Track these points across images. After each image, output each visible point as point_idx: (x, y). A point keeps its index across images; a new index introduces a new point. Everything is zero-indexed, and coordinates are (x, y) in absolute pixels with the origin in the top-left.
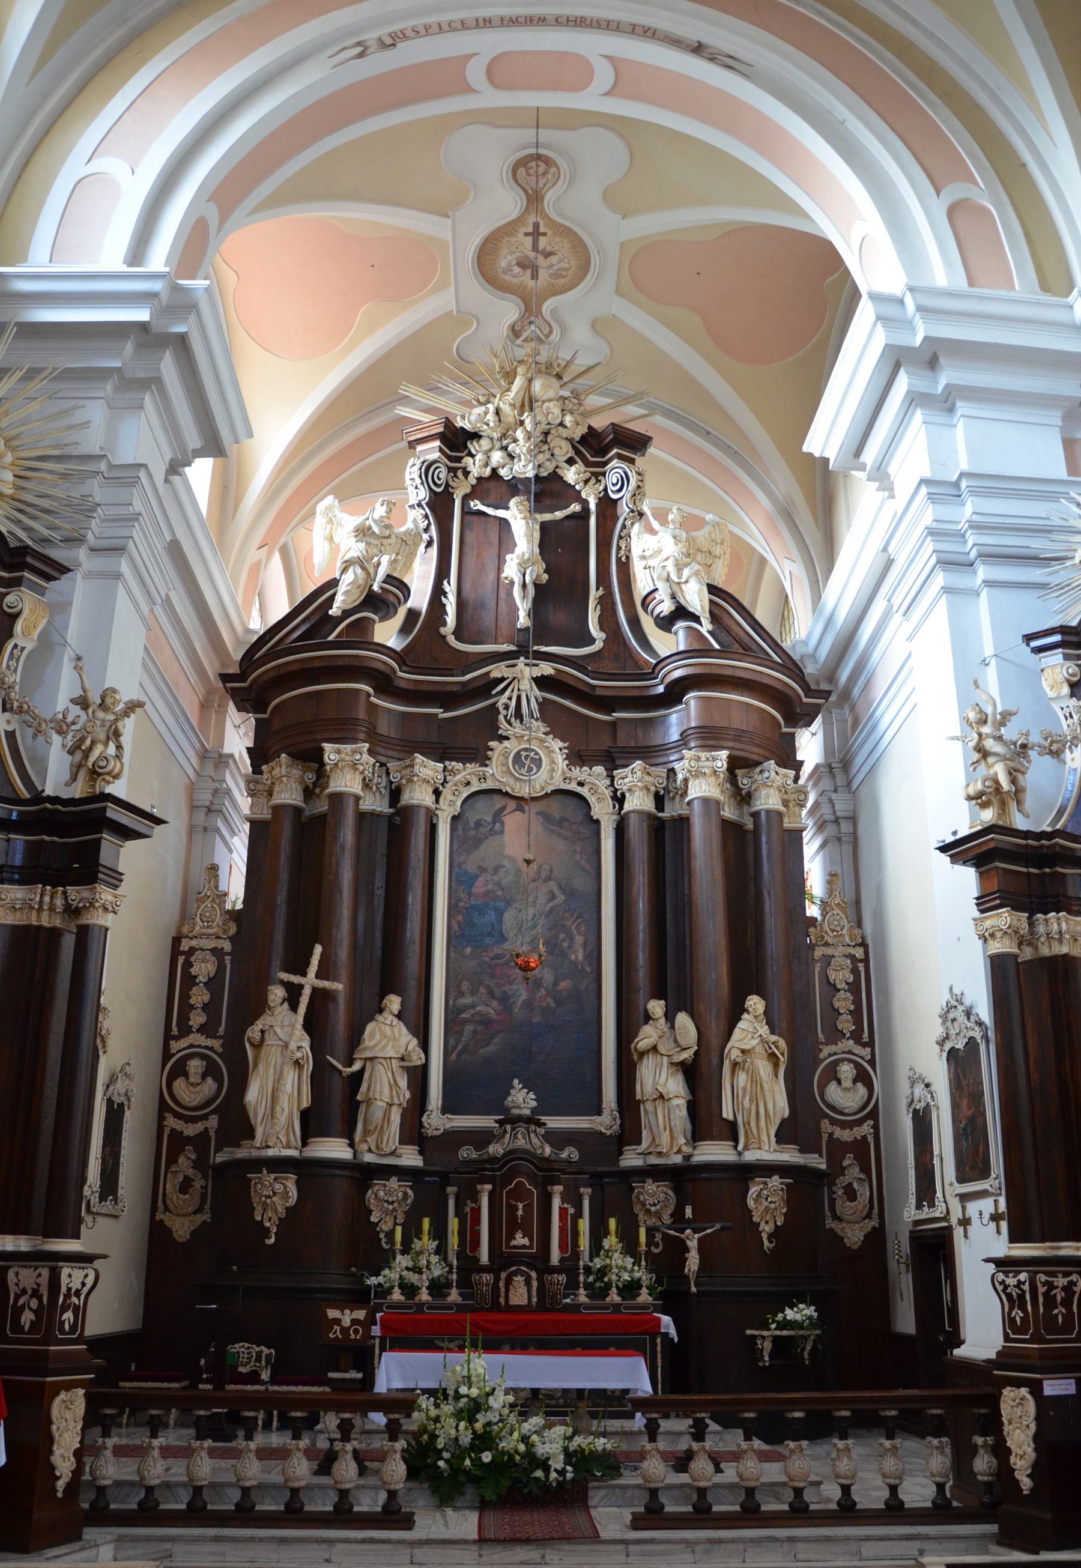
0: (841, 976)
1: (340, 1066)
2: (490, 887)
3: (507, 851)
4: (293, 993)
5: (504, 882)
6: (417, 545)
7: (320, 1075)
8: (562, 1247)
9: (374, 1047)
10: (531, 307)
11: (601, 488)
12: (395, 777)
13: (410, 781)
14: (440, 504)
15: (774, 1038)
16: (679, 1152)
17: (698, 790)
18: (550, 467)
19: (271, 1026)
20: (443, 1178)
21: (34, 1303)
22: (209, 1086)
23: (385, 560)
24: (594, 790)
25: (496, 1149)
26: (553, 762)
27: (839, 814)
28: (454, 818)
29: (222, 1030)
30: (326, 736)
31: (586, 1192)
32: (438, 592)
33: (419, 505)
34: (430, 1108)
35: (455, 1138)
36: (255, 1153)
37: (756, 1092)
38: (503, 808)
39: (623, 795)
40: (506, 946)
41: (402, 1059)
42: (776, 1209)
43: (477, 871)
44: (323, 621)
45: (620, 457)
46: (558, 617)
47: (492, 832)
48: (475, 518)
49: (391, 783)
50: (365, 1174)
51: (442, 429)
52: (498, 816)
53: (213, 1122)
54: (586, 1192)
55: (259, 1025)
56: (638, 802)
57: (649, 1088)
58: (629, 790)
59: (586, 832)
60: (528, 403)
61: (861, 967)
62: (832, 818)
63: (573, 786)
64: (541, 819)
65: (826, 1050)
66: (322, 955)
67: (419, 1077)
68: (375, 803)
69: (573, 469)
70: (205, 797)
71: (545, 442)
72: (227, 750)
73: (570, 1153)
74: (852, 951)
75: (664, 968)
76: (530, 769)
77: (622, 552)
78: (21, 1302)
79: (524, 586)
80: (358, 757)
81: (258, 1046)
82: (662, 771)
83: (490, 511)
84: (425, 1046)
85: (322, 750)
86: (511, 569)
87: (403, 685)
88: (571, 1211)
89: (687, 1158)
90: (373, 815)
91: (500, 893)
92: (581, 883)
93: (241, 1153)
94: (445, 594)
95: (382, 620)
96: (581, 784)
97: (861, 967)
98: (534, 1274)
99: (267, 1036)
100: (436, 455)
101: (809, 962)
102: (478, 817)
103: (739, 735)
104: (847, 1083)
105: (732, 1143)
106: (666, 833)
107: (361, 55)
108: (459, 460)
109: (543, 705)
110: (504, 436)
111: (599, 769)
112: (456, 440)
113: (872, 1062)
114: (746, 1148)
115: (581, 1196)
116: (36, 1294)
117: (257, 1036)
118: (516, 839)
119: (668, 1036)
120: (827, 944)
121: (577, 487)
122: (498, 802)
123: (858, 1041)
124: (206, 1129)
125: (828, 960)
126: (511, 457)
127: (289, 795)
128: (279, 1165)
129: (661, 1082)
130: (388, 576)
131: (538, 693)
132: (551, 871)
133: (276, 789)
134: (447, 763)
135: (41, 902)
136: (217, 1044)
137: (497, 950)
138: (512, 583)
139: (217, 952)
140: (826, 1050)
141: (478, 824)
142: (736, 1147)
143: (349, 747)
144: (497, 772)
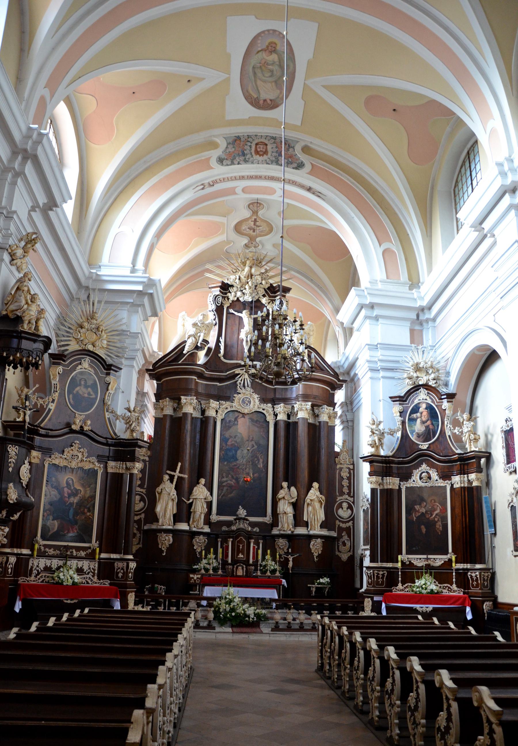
0: (345, 474)
1: (186, 501)
2: (233, 442)
3: (239, 431)
7: (180, 504)
8: (253, 558)
10: (252, 239)
12: (203, 406)
13: (208, 408)
14: (219, 310)
15: (321, 496)
16: (290, 530)
17: (301, 415)
18: (257, 297)
20: (217, 536)
21: (122, 571)
22: (142, 504)
24: (268, 412)
26: (255, 402)
28: (222, 419)
29: (145, 486)
31: (261, 541)
32: (218, 341)
33: (212, 311)
36: (159, 527)
38: (238, 416)
39: (277, 414)
41: (205, 499)
47: (234, 424)
48: (231, 315)
49: (202, 408)
50: (193, 534)
51: (220, 285)
52: (236, 419)
53: (143, 516)
54: (261, 541)
55: (161, 487)
56: (282, 417)
57: (281, 510)
58: (279, 413)
59: (265, 425)
63: (261, 410)
65: (339, 498)
67: (209, 505)
68: (197, 414)
69: (265, 299)
73: (257, 529)
74: (349, 466)
75: (287, 473)
76: (247, 404)
78: (118, 571)
79: (247, 341)
81: (160, 494)
82: (290, 407)
83: (236, 313)
84: (211, 494)
86: (242, 335)
87: (207, 376)
88: (256, 547)
89: (293, 532)
90: (196, 418)
92: (263, 442)
93: (154, 527)
94: (220, 342)
96: (263, 409)
98: (244, 566)
100: (218, 293)
101: (335, 469)
103: (315, 397)
106: (291, 426)
107: (203, 189)
108: (226, 294)
110: (242, 287)
111: (270, 405)
112: (225, 287)
113: (353, 503)
114: (311, 529)
116: (122, 569)
117: (160, 491)
118: (243, 427)
119: (288, 494)
120: (341, 464)
122: (237, 414)
124: (141, 518)
125: (341, 469)
126: (244, 294)
127: (169, 411)
129: (286, 508)
132: (253, 438)
133: (165, 409)
135: (120, 467)
136: (144, 491)
137: (235, 464)
140: (339, 498)
141: (230, 421)
144: (236, 405)
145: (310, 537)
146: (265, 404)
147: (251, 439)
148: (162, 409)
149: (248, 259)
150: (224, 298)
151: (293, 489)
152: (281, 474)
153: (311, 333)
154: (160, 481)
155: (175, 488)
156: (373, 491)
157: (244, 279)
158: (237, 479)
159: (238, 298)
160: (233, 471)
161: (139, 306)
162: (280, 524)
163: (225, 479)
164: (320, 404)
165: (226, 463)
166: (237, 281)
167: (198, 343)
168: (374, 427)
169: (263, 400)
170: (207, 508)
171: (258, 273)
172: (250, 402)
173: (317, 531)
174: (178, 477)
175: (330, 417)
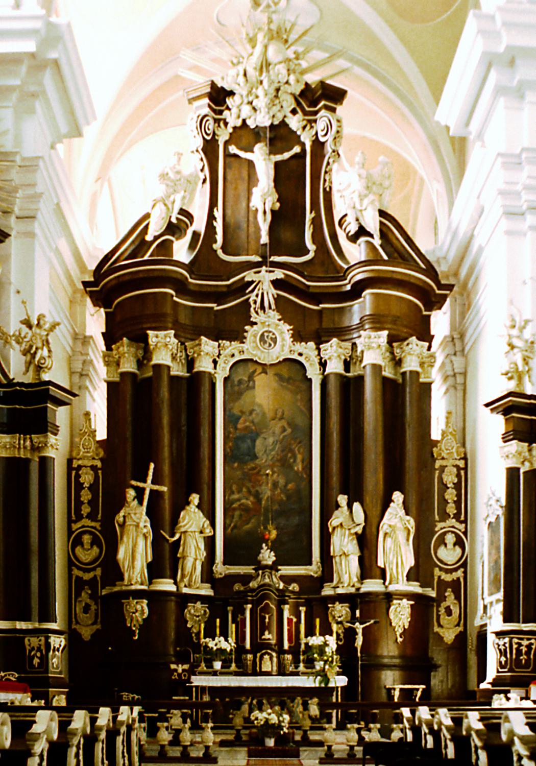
2: (248, 424)
3: (258, 400)
4: (140, 492)
5: (256, 421)
6: (196, 184)
7: (158, 543)
8: (290, 641)
9: (185, 526)
11: (314, 133)
13: (199, 355)
14: (209, 148)
16: (353, 586)
19: (129, 514)
20: (226, 599)
23: (178, 197)
25: (253, 584)
26: (283, 340)
27: (456, 371)
28: (226, 379)
30: (148, 325)
31: (303, 609)
32: (211, 217)
33: (197, 151)
34: (217, 561)
35: (231, 579)
36: (124, 588)
37: (397, 551)
38: (255, 371)
39: (326, 361)
40: (257, 462)
42: (404, 619)
43: (240, 414)
44: (141, 245)
45: (326, 107)
46: (287, 235)
48: (232, 159)
49: (187, 356)
50: (184, 600)
52: (251, 377)
54: (303, 609)
55: (122, 513)
56: (335, 367)
58: (329, 359)
59: (304, 386)
60: (265, 66)
61: (462, 472)
62: (451, 373)
63: (296, 357)
64: (277, 378)
66: (154, 469)
67: (210, 542)
68: (178, 370)
70: (78, 366)
71: (276, 97)
72: (88, 334)
73: (295, 587)
75: (348, 480)
76: (270, 345)
77: (327, 184)
79: (265, 212)
80: (168, 339)
81: (123, 525)
82: (348, 345)
84: (213, 524)
85: (147, 336)
86: (256, 202)
87: (192, 288)
88: (295, 620)
89: (358, 589)
91: (253, 428)
92: (300, 421)
93: (116, 589)
94: (215, 219)
95: (177, 239)
96: (300, 354)
97: (462, 472)
98: (274, 654)
99: (127, 520)
100: (207, 110)
102: (240, 378)
104: (450, 546)
105: (382, 581)
108: (221, 112)
109: (278, 299)
110: (250, 93)
111: (312, 344)
112: (219, 96)
114: (390, 583)
115: (300, 612)
117: (121, 519)
118: (264, 394)
119: (348, 518)
121: (298, 133)
122: (251, 367)
123: (457, 517)
126: (255, 109)
127: (129, 366)
128: (139, 594)
129: (344, 545)
130: (181, 209)
131: (275, 292)
132: (283, 414)
133: (122, 361)
134: (220, 341)
138: (257, 210)
139: (93, 468)
141: (240, 382)
142: (384, 583)
143: (161, 333)
144: (250, 348)
145: (389, 597)
146: (303, 343)
147: (279, 414)
148: (118, 364)
149: (259, 29)
150: (217, 121)
151: (357, 506)
152: (335, 480)
153: (386, 183)
154: (121, 502)
155: (148, 514)
156: (512, 473)
157: (252, 73)
158: (258, 496)
159: (244, 121)
160: (250, 481)
161: (34, 95)
162: (335, 575)
163: (236, 496)
164: (405, 335)
165: (236, 465)
166: (241, 79)
167: (171, 217)
168: (515, 332)
169: (298, 337)
170: (205, 549)
171: (280, 58)
172: (275, 340)
173: (401, 585)
174: (151, 491)
175: (422, 364)
